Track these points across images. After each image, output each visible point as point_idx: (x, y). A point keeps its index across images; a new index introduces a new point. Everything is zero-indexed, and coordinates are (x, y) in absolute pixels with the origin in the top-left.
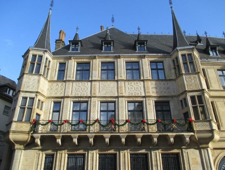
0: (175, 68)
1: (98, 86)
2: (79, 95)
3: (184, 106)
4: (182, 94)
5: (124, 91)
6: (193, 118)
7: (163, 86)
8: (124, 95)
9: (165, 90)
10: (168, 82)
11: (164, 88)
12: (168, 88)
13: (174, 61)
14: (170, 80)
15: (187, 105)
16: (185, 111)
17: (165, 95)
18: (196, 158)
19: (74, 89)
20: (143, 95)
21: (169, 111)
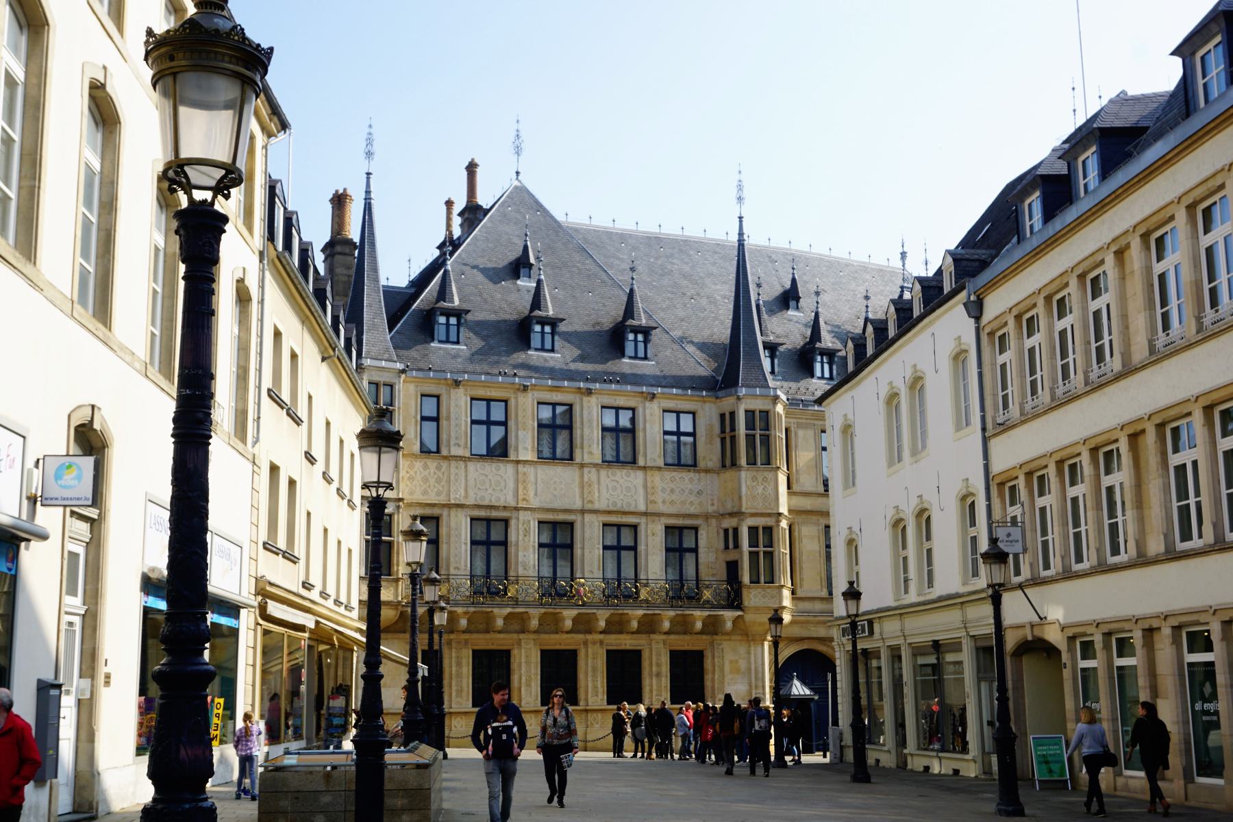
0: (723, 440)
1: (532, 478)
2: (486, 503)
3: (731, 545)
4: (732, 515)
5: (597, 494)
6: (746, 579)
7: (690, 486)
8: (597, 506)
9: (692, 498)
10: (703, 475)
11: (691, 492)
12: (699, 493)
13: (722, 416)
14: (707, 471)
15: (737, 545)
16: (732, 556)
17: (692, 510)
18: (737, 661)
19: (471, 482)
20: (642, 508)
21: (695, 550)
